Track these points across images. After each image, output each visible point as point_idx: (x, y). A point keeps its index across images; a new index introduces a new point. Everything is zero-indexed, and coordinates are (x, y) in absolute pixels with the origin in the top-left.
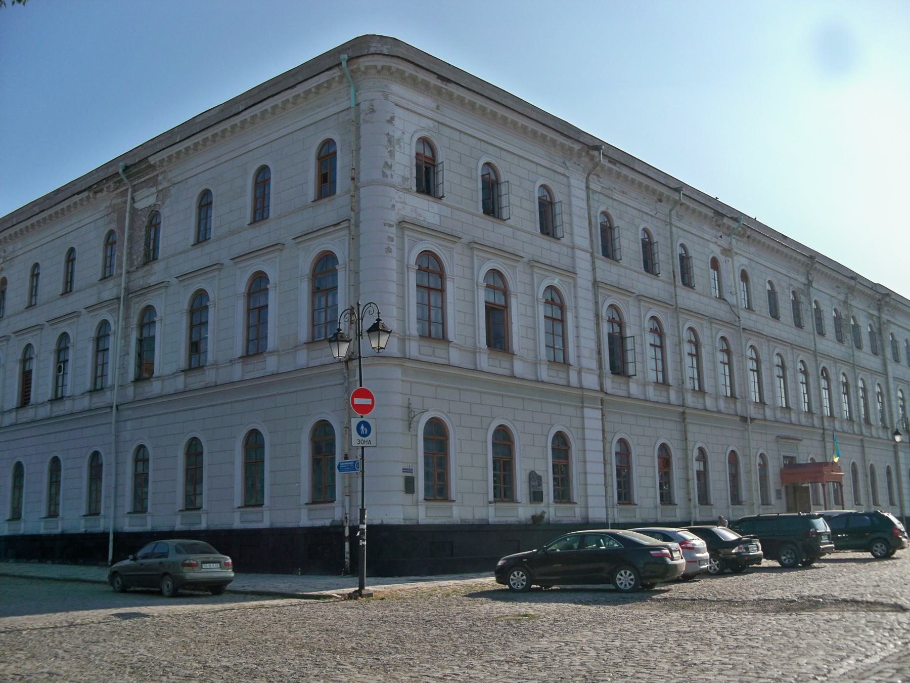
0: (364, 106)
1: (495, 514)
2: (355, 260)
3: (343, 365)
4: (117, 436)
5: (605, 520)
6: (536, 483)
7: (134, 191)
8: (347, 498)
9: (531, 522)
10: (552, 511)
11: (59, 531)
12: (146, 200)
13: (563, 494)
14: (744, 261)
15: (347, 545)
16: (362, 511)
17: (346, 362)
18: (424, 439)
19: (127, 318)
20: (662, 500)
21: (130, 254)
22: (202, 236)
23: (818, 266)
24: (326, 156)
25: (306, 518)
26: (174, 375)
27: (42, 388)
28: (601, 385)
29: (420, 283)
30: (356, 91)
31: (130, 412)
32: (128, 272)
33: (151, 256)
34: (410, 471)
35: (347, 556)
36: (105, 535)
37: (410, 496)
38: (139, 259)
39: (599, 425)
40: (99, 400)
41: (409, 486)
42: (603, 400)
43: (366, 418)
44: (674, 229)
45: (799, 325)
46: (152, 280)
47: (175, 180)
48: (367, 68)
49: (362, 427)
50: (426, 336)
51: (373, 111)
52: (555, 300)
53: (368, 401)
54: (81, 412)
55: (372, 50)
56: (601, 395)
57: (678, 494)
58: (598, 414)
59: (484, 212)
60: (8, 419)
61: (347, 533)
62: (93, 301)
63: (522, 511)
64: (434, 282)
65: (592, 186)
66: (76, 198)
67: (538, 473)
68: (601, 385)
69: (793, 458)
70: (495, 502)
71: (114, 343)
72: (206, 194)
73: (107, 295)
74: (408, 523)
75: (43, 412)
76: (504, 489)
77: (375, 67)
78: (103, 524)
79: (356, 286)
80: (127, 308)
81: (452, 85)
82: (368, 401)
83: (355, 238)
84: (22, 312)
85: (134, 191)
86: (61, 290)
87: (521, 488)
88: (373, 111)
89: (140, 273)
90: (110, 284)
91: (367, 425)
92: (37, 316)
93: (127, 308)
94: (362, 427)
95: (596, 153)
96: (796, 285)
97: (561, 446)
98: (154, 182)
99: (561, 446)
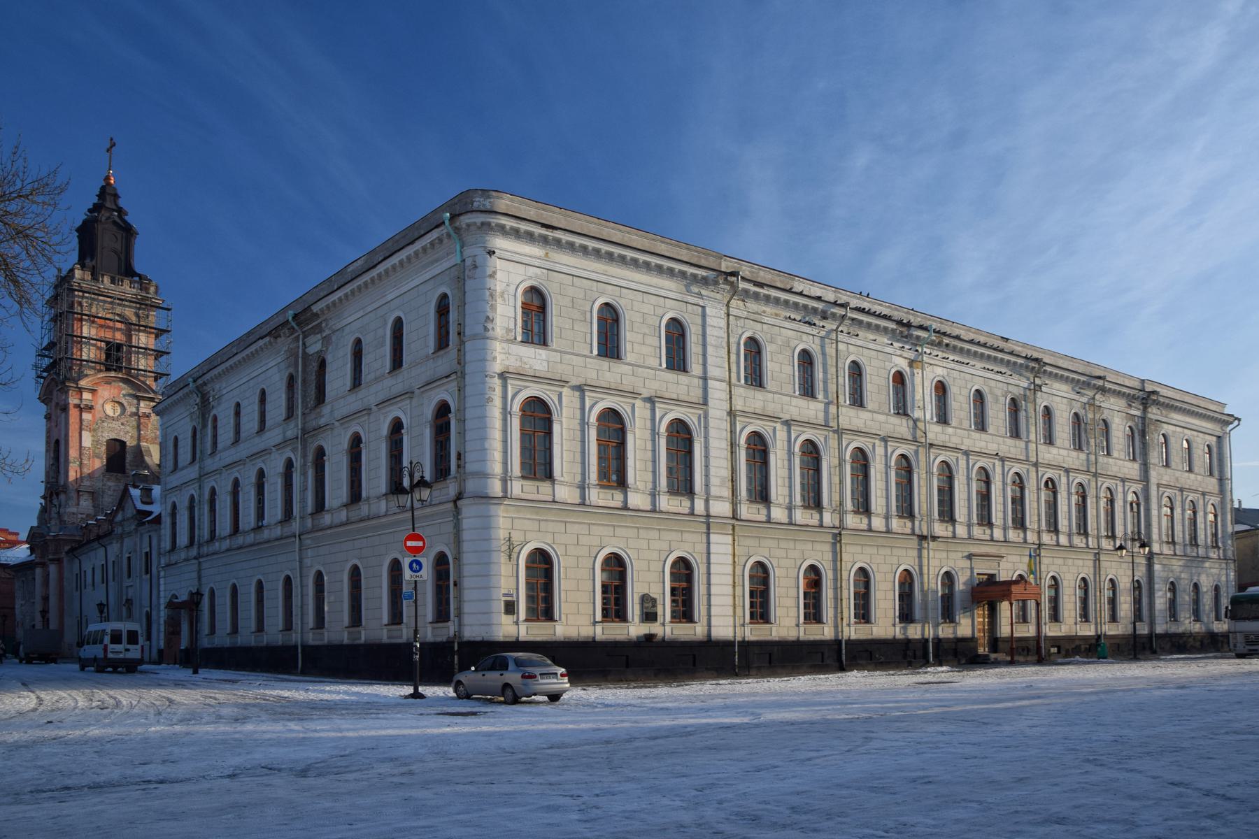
0: (469, 262)
7: (305, 337)
12: (314, 346)
14: (939, 371)
16: (416, 632)
19: (304, 456)
20: (805, 618)
21: (304, 397)
22: (357, 382)
23: (1048, 369)
24: (443, 309)
25: (384, 636)
30: (462, 247)
32: (303, 414)
33: (321, 397)
38: (312, 403)
40: (287, 530)
44: (841, 346)
45: (1016, 433)
46: (322, 421)
51: (475, 267)
54: (277, 539)
62: (279, 439)
65: (733, 311)
71: (297, 478)
72: (358, 342)
73: (290, 434)
80: (304, 448)
84: (229, 448)
85: (305, 337)
86: (256, 427)
88: (475, 267)
89: (313, 416)
90: (292, 425)
92: (243, 451)
93: (304, 448)
95: (734, 279)
98: (318, 329)
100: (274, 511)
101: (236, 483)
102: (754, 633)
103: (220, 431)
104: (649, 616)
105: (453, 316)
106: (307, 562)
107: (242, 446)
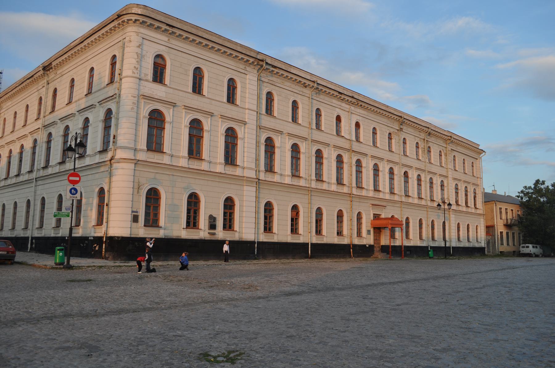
1: (185, 234)
2: (118, 113)
3: (109, 163)
4: (35, 192)
5: (253, 240)
6: (212, 220)
11: (14, 236)
13: (228, 225)
17: (110, 160)
18: (147, 198)
26: (56, 165)
27: (14, 171)
31: (40, 182)
34: (137, 212)
35: (104, 250)
36: (28, 238)
37: (135, 224)
41: (135, 219)
43: (76, 186)
47: (63, 74)
48: (128, 20)
49: (73, 190)
50: (150, 149)
52: (231, 134)
53: (78, 179)
55: (133, 12)
59: (193, 91)
60: (3, 184)
61: (104, 240)
63: (202, 233)
64: (155, 123)
66: (28, 81)
67: (214, 216)
70: (186, 228)
74: (132, 236)
75: (14, 181)
76: (192, 221)
77: (131, 20)
78: (28, 234)
79: (117, 125)
81: (175, 29)
82: (78, 179)
83: (118, 103)
84: (9, 135)
87: (203, 222)
91: (76, 190)
94: (73, 190)
96: (392, 130)
97: (229, 204)
99: (229, 204)
100: (26, 167)
101: (11, 151)
103: (6, 126)
104: (213, 226)
105: (118, 66)
106: (38, 192)
107: (15, 134)
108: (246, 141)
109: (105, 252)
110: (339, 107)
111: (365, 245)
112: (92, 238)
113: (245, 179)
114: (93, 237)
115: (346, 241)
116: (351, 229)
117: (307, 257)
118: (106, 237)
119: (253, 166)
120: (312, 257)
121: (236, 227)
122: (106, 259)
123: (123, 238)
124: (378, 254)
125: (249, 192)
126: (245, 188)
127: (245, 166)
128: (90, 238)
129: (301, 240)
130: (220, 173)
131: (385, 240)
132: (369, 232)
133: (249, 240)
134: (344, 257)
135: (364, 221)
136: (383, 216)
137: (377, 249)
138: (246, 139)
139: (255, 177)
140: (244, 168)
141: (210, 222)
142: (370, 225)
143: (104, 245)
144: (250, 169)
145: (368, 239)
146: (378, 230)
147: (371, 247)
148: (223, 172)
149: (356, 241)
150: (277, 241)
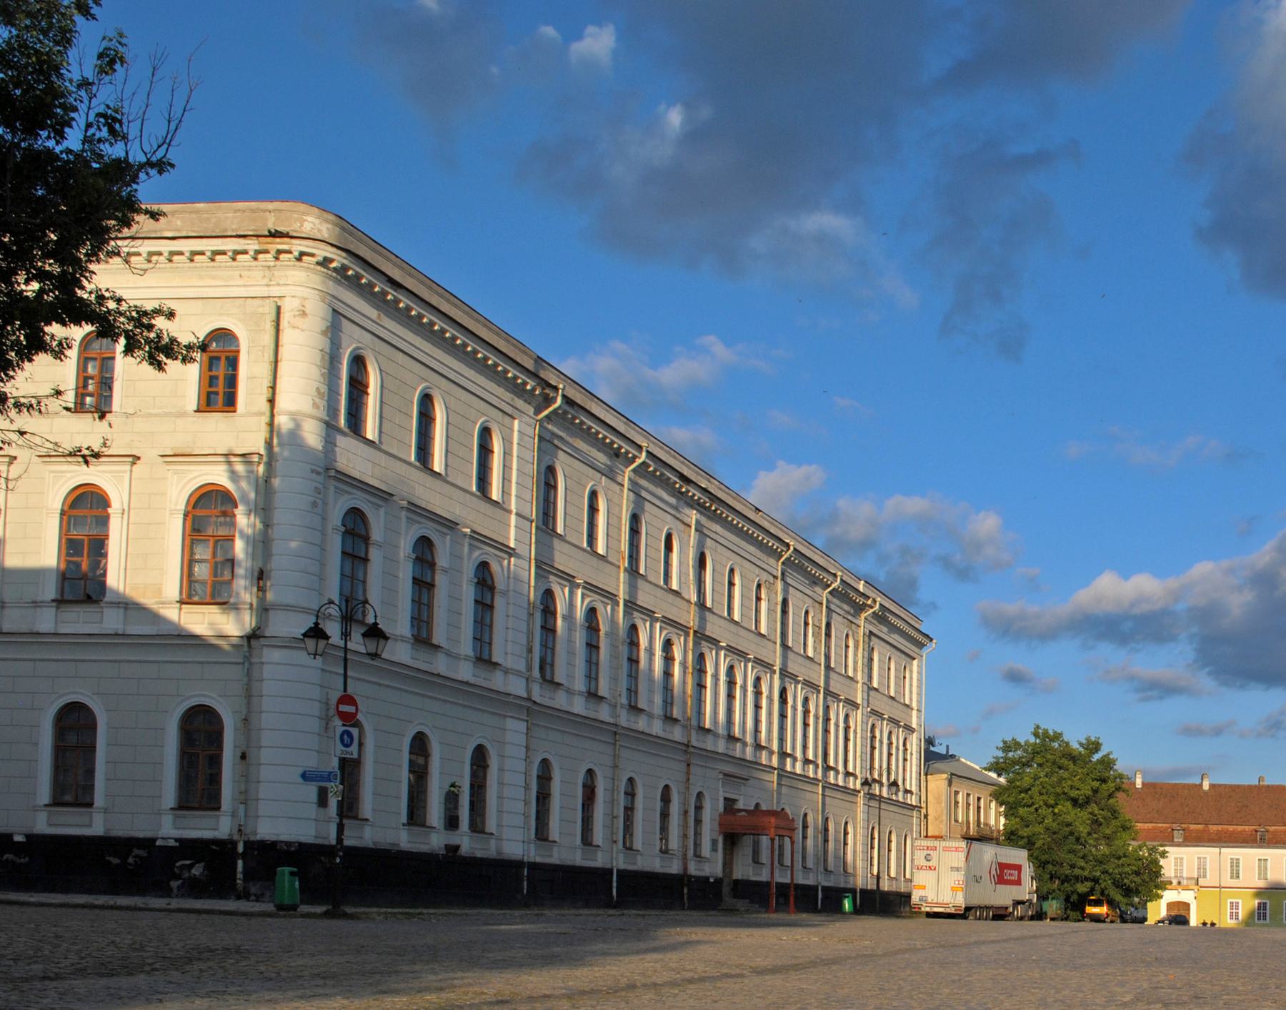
1: (405, 840)
8: (242, 807)
9: (443, 852)
10: (467, 843)
15: (240, 863)
28: (529, 691)
29: (349, 550)
35: (240, 876)
39: (522, 740)
42: (530, 709)
56: (529, 704)
57: (599, 836)
58: (522, 726)
68: (529, 691)
69: (734, 801)
87: (435, 812)
102: (534, 854)
108: (511, 601)
109: (245, 879)
110: (673, 512)
111: (708, 878)
112: (172, 843)
113: (511, 699)
114: (176, 840)
115: (675, 868)
116: (685, 836)
117: (609, 904)
118: (246, 843)
119: (522, 666)
120: (616, 906)
121: (491, 825)
122: (245, 895)
123: (301, 845)
124: (728, 900)
125: (515, 729)
126: (511, 724)
127: (509, 666)
128: (158, 843)
129: (599, 861)
130: (467, 683)
131: (744, 870)
132: (714, 842)
133: (513, 858)
134: (669, 907)
135: (707, 815)
136: (740, 805)
137: (726, 890)
138: (511, 594)
139: (525, 695)
140: (507, 672)
141: (447, 809)
142: (716, 827)
143: (240, 863)
144: (518, 673)
145: (712, 866)
146: (731, 840)
147: (719, 881)
148: (472, 680)
149: (693, 870)
150: (558, 862)
